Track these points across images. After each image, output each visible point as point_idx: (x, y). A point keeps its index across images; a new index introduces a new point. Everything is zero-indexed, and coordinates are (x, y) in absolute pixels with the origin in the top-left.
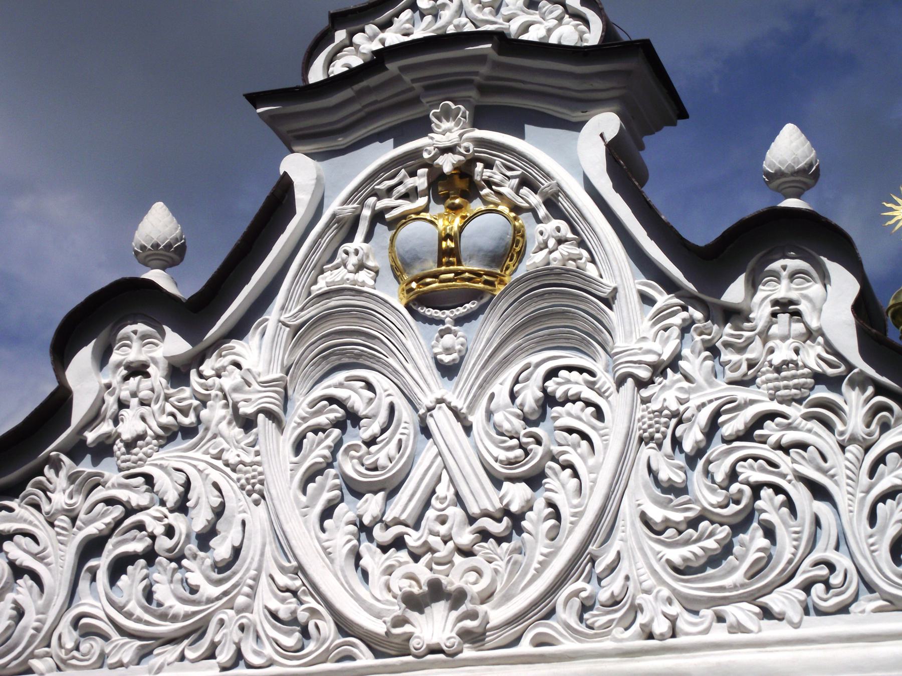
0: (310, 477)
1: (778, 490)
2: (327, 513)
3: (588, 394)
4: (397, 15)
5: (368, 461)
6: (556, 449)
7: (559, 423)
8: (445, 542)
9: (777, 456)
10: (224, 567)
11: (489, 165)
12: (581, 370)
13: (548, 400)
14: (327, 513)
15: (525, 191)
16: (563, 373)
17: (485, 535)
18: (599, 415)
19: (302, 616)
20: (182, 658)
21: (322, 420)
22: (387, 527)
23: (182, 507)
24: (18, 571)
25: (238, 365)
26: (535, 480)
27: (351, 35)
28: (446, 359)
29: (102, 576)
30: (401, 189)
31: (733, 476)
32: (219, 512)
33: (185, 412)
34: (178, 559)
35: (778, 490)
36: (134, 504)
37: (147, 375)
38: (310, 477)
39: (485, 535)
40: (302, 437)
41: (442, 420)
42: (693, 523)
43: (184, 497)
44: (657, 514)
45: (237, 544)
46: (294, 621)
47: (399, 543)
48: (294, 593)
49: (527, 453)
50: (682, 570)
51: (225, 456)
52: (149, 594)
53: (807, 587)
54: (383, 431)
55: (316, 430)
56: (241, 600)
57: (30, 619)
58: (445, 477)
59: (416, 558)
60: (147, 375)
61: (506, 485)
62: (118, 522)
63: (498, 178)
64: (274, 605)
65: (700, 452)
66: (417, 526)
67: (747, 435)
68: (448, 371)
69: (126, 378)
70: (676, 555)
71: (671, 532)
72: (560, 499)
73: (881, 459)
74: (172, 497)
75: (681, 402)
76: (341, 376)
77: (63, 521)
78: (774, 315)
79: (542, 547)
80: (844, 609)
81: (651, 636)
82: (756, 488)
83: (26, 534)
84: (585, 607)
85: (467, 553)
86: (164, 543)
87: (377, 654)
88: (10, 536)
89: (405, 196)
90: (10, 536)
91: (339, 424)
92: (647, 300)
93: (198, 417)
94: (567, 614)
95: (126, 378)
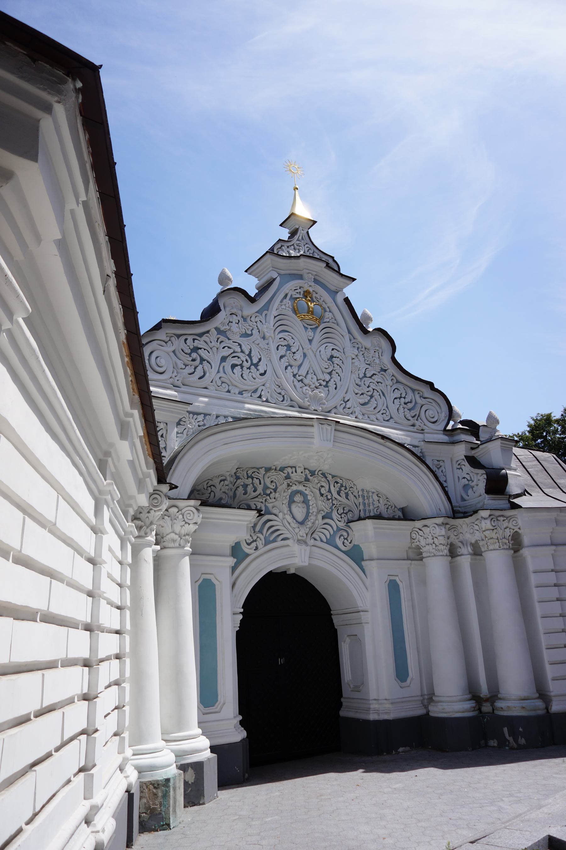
0: (281, 357)
1: (378, 392)
2: (286, 368)
3: (340, 357)
4: (291, 246)
5: (295, 358)
6: (335, 369)
7: (336, 362)
8: (313, 384)
9: (376, 383)
10: (261, 375)
11: (316, 293)
12: (338, 351)
13: (332, 357)
14: (286, 368)
15: (324, 303)
16: (335, 350)
17: (320, 385)
18: (343, 363)
19: (283, 394)
20: (251, 396)
21: (283, 344)
22: (299, 376)
23: (249, 355)
24: (202, 360)
25: (261, 322)
26: (330, 373)
27: (282, 246)
28: (311, 338)
29: (228, 369)
30: (297, 291)
31: (368, 387)
32: (260, 360)
33: (248, 329)
34: (249, 368)
35: (378, 392)
36: (236, 350)
37: (237, 316)
38: (281, 357)
39: (320, 385)
40: (278, 346)
41: (310, 354)
42: (362, 394)
43: (250, 352)
44: (357, 391)
45: (265, 370)
46: (280, 394)
47: (301, 381)
48: (279, 387)
49: (329, 368)
50: (362, 405)
51: (260, 345)
52: (242, 375)
53: (382, 414)
54: (297, 351)
55: (282, 346)
56: (267, 385)
57: (207, 374)
58: (311, 368)
59: (306, 386)
60: (237, 316)
61: (325, 374)
62: (231, 354)
63: (319, 298)
64: (276, 389)
65: (363, 377)
66: (305, 377)
67: (370, 377)
68: (310, 341)
69: (231, 314)
70: (362, 401)
71: (359, 395)
72: (336, 380)
73: (394, 390)
74: (247, 353)
75: (360, 365)
76: (287, 333)
77: (215, 349)
78: (375, 352)
79: (335, 391)
80: (388, 421)
81: (356, 418)
82: (374, 389)
83: (205, 349)
84: (344, 408)
85: (317, 388)
86: (245, 364)
87: (300, 407)
88: (201, 349)
89: (298, 293)
90: (201, 349)
91: (285, 346)
92: (350, 340)
93: (251, 331)
94: (340, 409)
95: (231, 314)
